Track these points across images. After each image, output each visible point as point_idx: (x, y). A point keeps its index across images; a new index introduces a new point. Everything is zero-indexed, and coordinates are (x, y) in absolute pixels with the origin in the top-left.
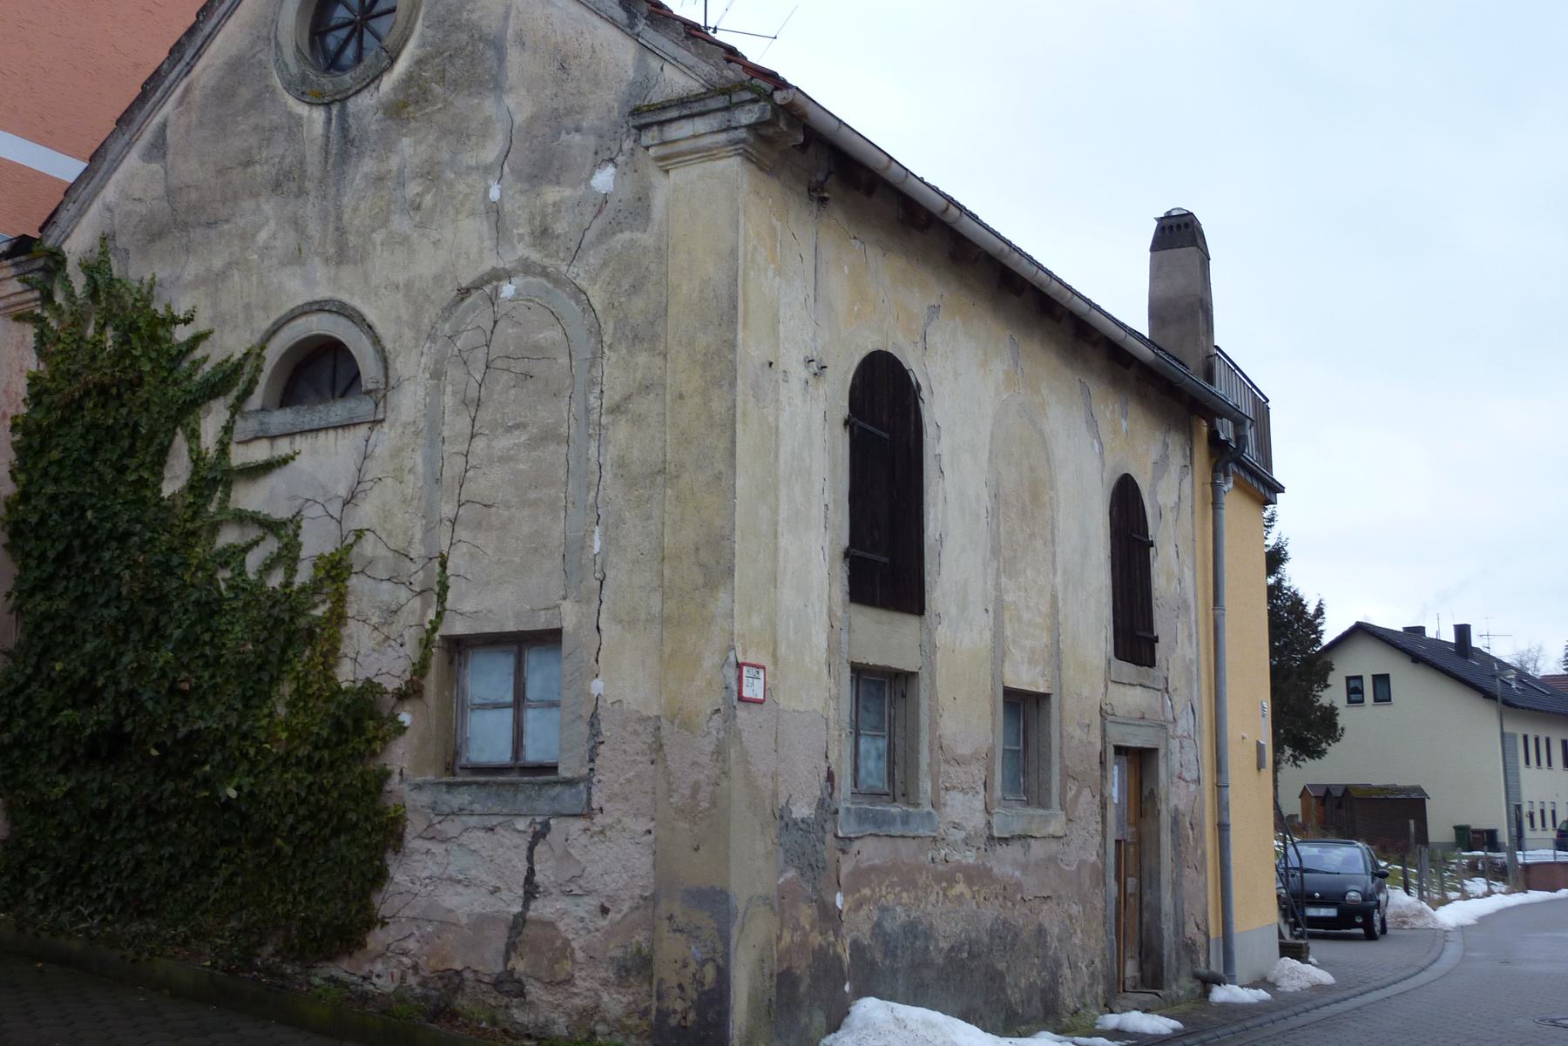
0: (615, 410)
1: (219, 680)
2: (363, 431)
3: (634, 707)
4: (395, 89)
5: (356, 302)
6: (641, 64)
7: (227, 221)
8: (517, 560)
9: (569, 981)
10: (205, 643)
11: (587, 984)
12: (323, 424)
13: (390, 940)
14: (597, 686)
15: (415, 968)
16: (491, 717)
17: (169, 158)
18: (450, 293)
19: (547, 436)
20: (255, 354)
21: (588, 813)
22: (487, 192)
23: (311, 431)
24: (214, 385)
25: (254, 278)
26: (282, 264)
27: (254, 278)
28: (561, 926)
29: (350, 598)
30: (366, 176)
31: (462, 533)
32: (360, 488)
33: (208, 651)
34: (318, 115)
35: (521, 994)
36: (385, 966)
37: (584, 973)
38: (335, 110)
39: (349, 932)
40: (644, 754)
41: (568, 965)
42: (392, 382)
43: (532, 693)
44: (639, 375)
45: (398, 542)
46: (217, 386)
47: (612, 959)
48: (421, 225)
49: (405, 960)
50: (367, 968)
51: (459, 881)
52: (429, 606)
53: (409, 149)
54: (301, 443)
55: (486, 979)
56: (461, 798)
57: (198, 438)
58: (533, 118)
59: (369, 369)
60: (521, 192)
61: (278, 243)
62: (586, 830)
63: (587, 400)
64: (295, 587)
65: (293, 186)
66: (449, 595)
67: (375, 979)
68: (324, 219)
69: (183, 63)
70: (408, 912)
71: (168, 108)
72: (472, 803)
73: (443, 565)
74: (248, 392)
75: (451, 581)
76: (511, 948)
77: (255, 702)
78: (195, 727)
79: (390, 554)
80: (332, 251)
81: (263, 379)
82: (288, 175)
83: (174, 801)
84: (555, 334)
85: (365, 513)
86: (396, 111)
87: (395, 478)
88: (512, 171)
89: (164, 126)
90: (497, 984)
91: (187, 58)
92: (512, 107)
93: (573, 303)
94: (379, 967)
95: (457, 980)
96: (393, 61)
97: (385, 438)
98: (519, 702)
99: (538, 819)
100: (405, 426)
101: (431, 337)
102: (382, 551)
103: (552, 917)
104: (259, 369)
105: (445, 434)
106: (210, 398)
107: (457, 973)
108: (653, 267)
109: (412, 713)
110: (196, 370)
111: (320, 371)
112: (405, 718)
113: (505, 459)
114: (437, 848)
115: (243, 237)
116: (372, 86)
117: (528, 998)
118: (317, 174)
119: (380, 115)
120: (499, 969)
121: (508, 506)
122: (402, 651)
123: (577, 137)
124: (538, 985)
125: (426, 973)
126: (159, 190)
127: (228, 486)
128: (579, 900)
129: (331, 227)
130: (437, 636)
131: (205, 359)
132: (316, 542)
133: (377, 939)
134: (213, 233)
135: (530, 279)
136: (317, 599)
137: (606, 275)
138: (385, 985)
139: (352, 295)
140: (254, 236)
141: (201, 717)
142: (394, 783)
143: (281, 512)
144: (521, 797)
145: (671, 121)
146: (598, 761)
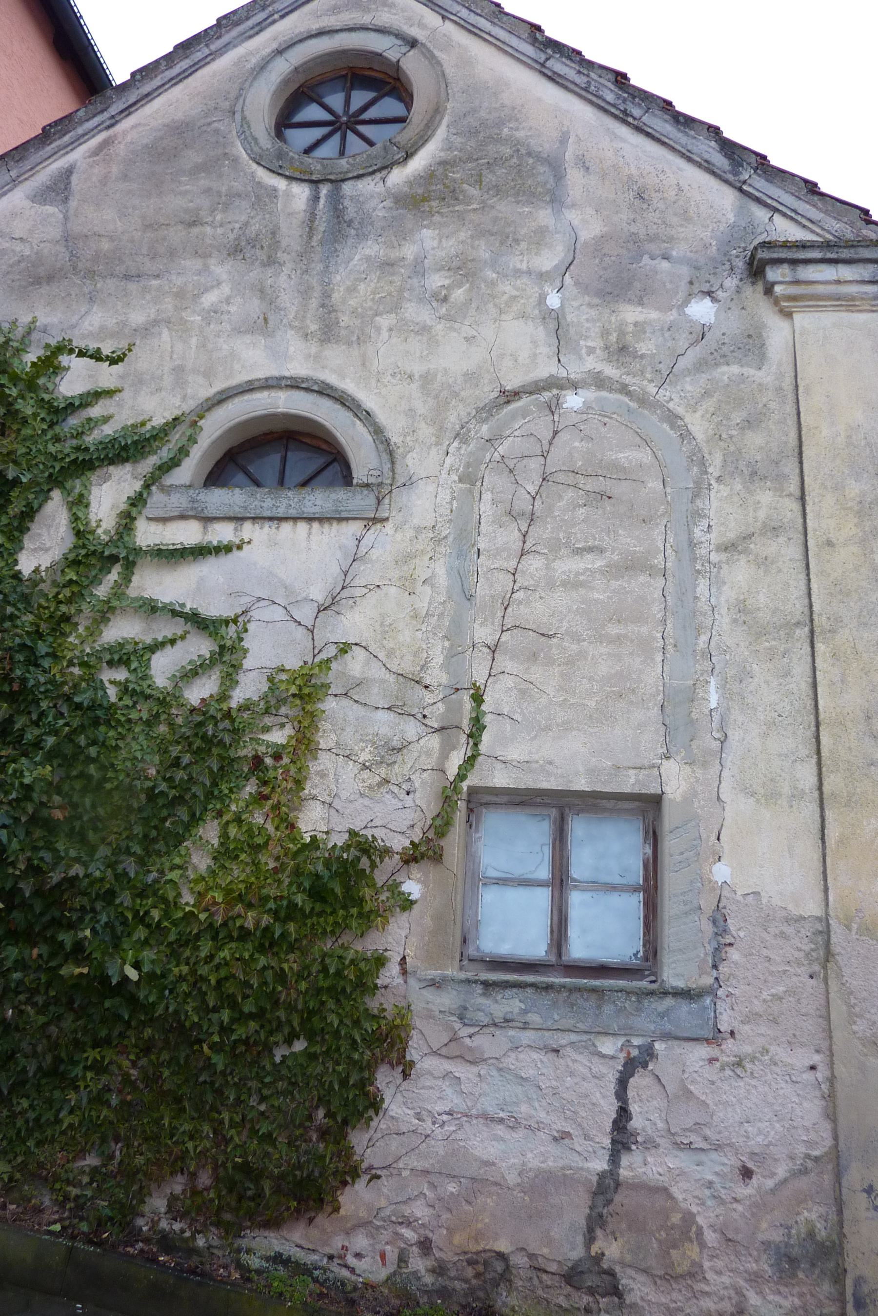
0: (728, 547)
1: (101, 811)
2: (355, 528)
3: (777, 901)
4: (410, 183)
5: (349, 386)
6: (740, 211)
7: (157, 276)
8: (592, 704)
9: (695, 1273)
10: (90, 760)
11: (726, 1280)
12: (293, 512)
13: (383, 1203)
14: (721, 872)
15: (425, 1246)
16: (515, 896)
17: (73, 203)
18: (488, 393)
19: (632, 565)
20: (187, 423)
21: (715, 1037)
22: (542, 298)
23: (271, 519)
24: (125, 448)
25: (194, 341)
26: (238, 331)
27: (194, 341)
28: (675, 1191)
29: (324, 725)
30: (368, 258)
31: (504, 662)
32: (345, 593)
33: (92, 769)
34: (301, 193)
35: (616, 1292)
36: (364, 1236)
37: (719, 1264)
38: (324, 190)
39: (312, 1191)
40: (799, 964)
41: (693, 1251)
42: (400, 480)
43: (579, 870)
44: (762, 515)
45: (407, 666)
46: (125, 450)
47: (767, 1244)
48: (449, 318)
49: (408, 1234)
50: (338, 1242)
51: (501, 1121)
52: (454, 748)
53: (429, 241)
54: (248, 530)
55: (553, 1268)
56: (510, 1004)
57: (87, 506)
58: (603, 238)
59: (363, 458)
60: (590, 305)
61: (233, 309)
62: (712, 1060)
63: (690, 532)
64: (234, 704)
65: (262, 255)
66: (486, 737)
67: (351, 1260)
68: (305, 293)
69: (106, 115)
70: (414, 1162)
71: (78, 155)
72: (525, 1012)
73: (478, 698)
74: (173, 463)
75: (487, 719)
76: (596, 1223)
77: (160, 846)
78: (72, 873)
79: (392, 679)
80: (313, 327)
81: (196, 452)
82: (253, 242)
83: (16, 976)
84: (644, 456)
85: (353, 624)
86: (416, 202)
87: (403, 587)
88: (577, 284)
89: (69, 172)
90: (572, 1277)
91: (114, 110)
92: (575, 223)
93: (666, 426)
94: (360, 1242)
95: (499, 1267)
96: (408, 156)
97: (385, 543)
98: (560, 881)
99: (636, 1041)
100: (419, 530)
101: (462, 436)
102: (376, 672)
103: (664, 1181)
104: (192, 440)
105: (481, 546)
106: (112, 462)
107: (501, 1256)
108: (773, 405)
109: (424, 883)
110: (91, 429)
111: (286, 454)
112: (412, 888)
113: (572, 584)
114: (459, 1070)
115: (180, 294)
116: (378, 175)
117: (629, 1299)
118: (297, 247)
119: (388, 203)
120: (577, 1253)
121: (576, 638)
122: (409, 801)
123: (665, 265)
124: (641, 1278)
125: (448, 1256)
126: (55, 232)
127: (129, 566)
128: (703, 1157)
129: (314, 303)
130: (465, 785)
131: (106, 419)
132: (269, 650)
133: (356, 1199)
134: (132, 286)
135: (604, 394)
136: (268, 720)
137: (710, 404)
138: (370, 1269)
139: (343, 377)
140: (196, 297)
141: (77, 860)
142: (390, 974)
143: (213, 609)
144: (608, 1009)
145: (807, 262)
146: (723, 968)
